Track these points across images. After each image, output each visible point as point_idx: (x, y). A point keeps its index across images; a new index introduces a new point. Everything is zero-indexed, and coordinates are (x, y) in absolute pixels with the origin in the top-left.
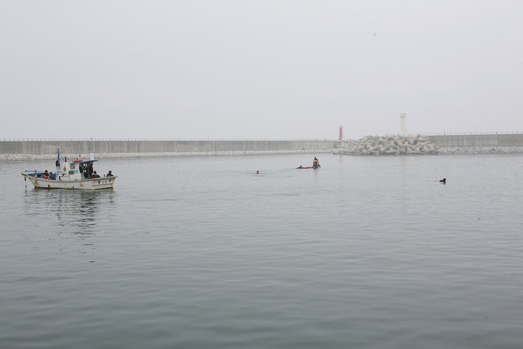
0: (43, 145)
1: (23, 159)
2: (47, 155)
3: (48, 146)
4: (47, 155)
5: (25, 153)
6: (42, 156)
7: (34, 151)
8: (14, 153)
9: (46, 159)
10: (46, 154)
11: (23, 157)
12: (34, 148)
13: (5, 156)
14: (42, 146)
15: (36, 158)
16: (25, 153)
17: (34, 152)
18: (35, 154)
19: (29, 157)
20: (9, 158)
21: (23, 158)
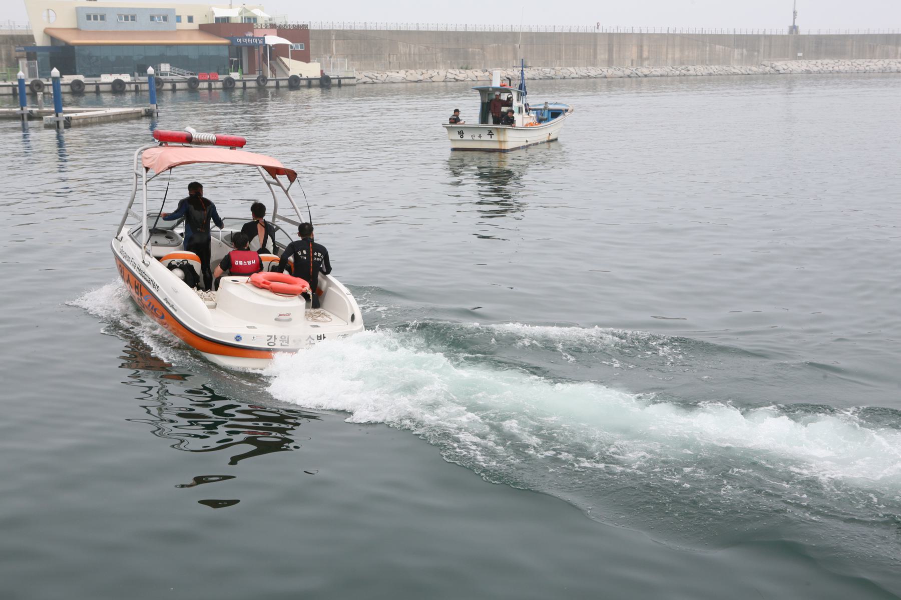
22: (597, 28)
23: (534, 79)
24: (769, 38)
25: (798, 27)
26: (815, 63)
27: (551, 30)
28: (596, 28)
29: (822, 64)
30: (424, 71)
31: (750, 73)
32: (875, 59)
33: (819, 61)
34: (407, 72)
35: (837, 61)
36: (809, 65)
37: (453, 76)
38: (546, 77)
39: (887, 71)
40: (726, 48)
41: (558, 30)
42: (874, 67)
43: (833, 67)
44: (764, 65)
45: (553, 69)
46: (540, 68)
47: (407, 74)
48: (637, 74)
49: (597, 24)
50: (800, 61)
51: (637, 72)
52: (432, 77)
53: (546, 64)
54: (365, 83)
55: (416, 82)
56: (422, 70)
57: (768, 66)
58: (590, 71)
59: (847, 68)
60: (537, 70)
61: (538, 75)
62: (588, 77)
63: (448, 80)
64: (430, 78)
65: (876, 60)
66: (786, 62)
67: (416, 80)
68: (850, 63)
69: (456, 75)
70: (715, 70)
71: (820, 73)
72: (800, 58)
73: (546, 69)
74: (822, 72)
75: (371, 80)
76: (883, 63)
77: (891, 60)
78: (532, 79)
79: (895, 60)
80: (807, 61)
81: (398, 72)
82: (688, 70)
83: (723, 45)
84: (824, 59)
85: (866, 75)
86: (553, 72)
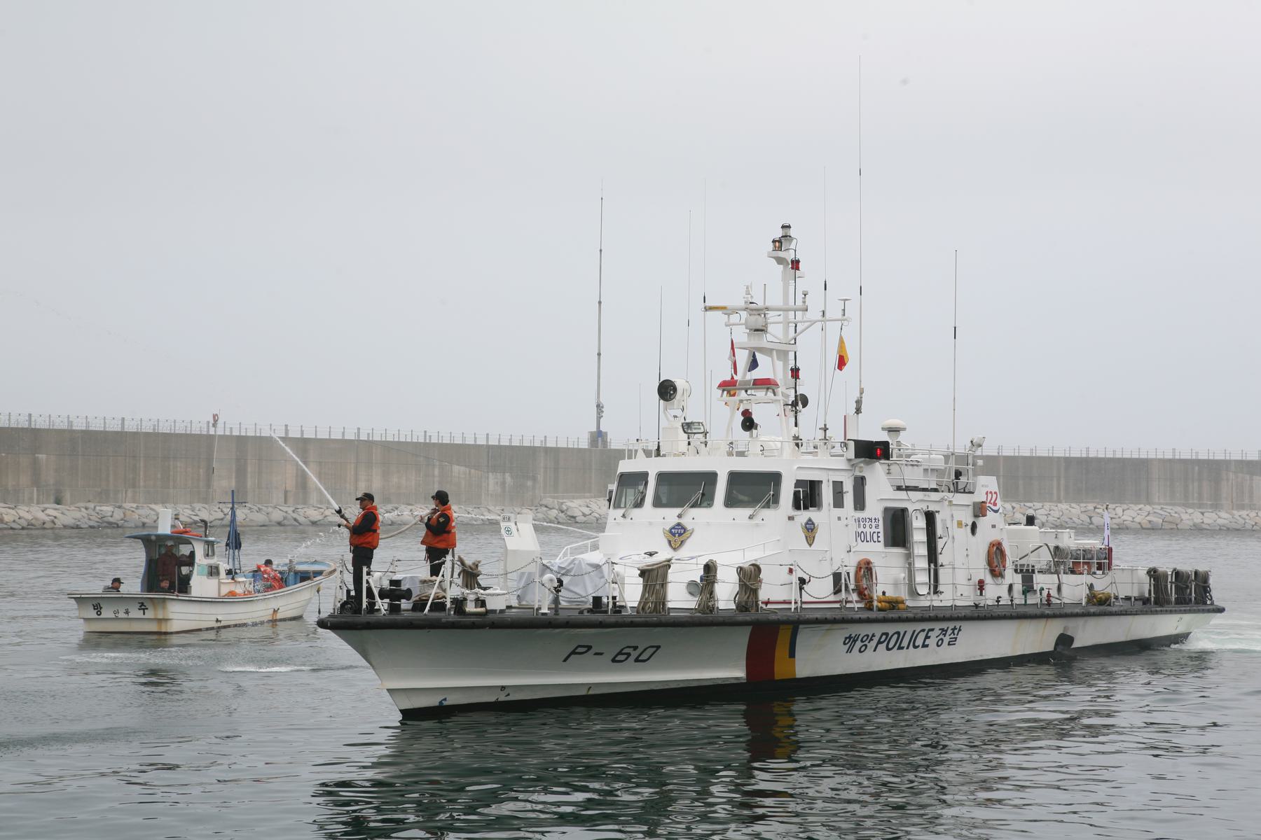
0: (1231, 475)
1: (1149, 526)
2: (1244, 513)
3: (1251, 480)
4: (1241, 513)
5: (1159, 504)
6: (1223, 514)
7: (1196, 495)
8: (1120, 500)
9: (1238, 527)
10: (1242, 507)
11: (1149, 518)
12: (1196, 484)
13: (1083, 509)
14: (1228, 480)
15: (1198, 521)
16: (1162, 501)
17: (1195, 502)
18: (1200, 506)
19: (1170, 519)
20: (1096, 520)
21: (1150, 522)
22: (214, 425)
23: (78, 527)
27: (114, 426)
28: (211, 425)
38: (105, 524)
41: (130, 427)
45: (120, 507)
46: (91, 505)
48: (295, 520)
51: (295, 515)
53: (103, 497)
57: (553, 508)
58: (199, 513)
60: (83, 509)
61: (86, 520)
62: (194, 525)
73: (104, 508)
78: (73, 528)
86: (118, 515)
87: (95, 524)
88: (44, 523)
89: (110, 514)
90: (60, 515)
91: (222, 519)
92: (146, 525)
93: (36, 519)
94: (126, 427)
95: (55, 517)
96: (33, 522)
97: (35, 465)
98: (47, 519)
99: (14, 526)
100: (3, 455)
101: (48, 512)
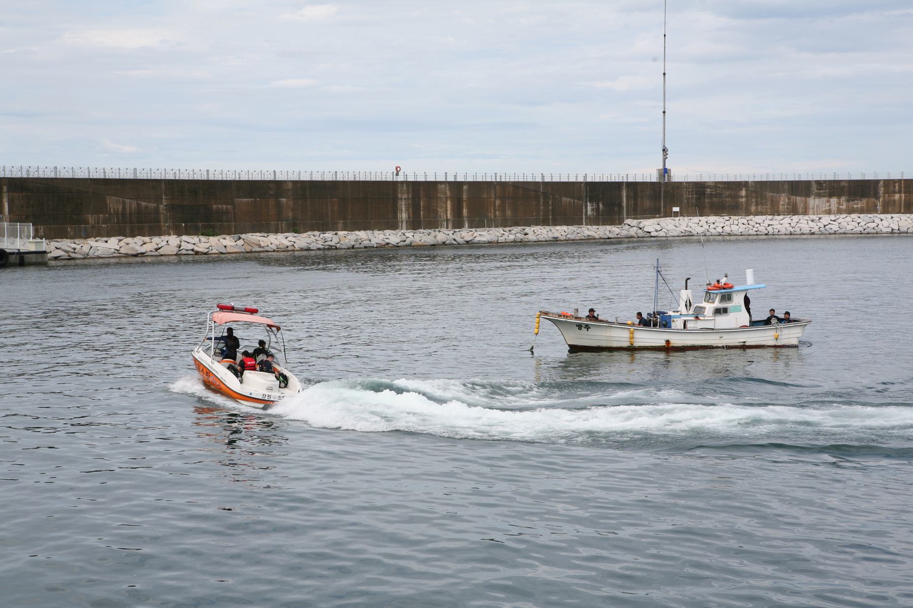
22: (397, 174)
24: (634, 187)
25: (670, 170)
26: (698, 222)
28: (395, 174)
29: (707, 222)
30: (147, 239)
31: (611, 236)
32: (779, 215)
33: (704, 219)
34: (120, 241)
35: (727, 218)
36: (690, 224)
37: (190, 247)
39: (795, 233)
40: (576, 201)
42: (779, 227)
43: (723, 227)
44: (629, 225)
47: (122, 243)
49: (396, 169)
50: (677, 219)
51: (454, 237)
52: (159, 248)
54: (56, 258)
55: (136, 255)
56: (142, 238)
58: (389, 237)
59: (742, 229)
60: (312, 237)
63: (184, 252)
64: (157, 250)
65: (781, 217)
66: (658, 220)
67: (135, 253)
68: (745, 221)
69: (194, 244)
70: (563, 233)
71: (705, 235)
72: (676, 214)
74: (708, 234)
75: (66, 254)
76: (790, 221)
77: (800, 217)
79: (806, 217)
80: (686, 219)
81: (106, 242)
82: (526, 234)
83: (571, 198)
84: (709, 216)
85: (770, 237)
87: (322, 247)
88: (288, 247)
89: (330, 239)
90: (298, 241)
91: (405, 241)
92: (355, 247)
93: (283, 244)
94: (338, 177)
95: (295, 242)
96: (280, 246)
97: (279, 205)
98: (289, 244)
99: (267, 249)
100: (258, 199)
101: (289, 239)
